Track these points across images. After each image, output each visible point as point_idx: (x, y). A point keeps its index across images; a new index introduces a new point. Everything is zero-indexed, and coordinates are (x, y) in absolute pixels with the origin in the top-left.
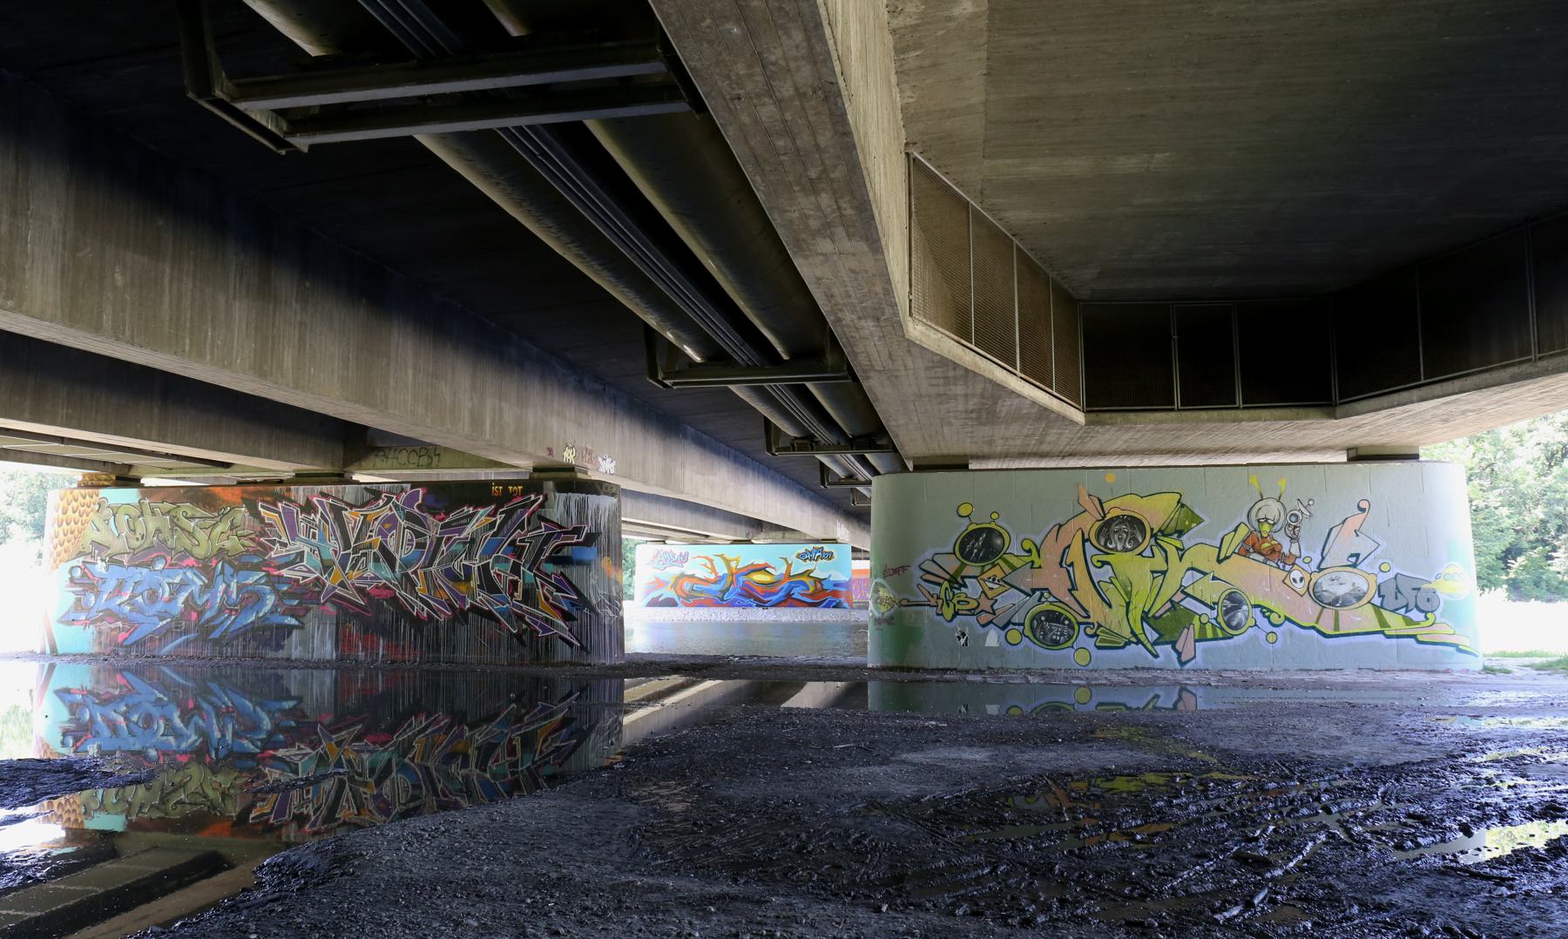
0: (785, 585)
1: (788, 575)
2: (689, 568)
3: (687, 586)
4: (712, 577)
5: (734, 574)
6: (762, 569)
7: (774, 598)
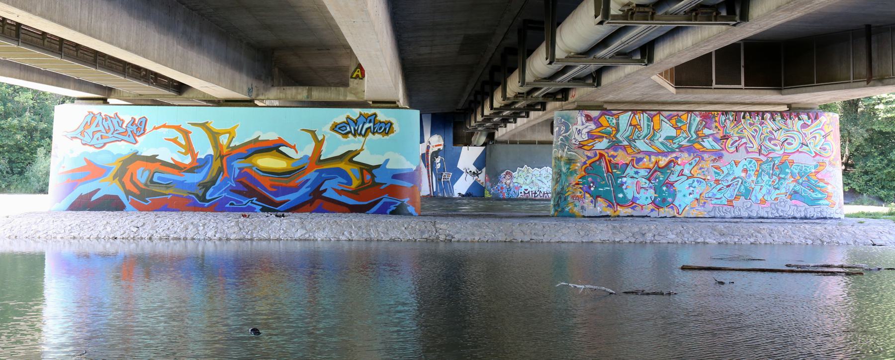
0: (312, 175)
1: (316, 159)
2: (146, 146)
3: (142, 176)
4: (187, 160)
5: (225, 157)
6: (274, 148)
7: (292, 197)
